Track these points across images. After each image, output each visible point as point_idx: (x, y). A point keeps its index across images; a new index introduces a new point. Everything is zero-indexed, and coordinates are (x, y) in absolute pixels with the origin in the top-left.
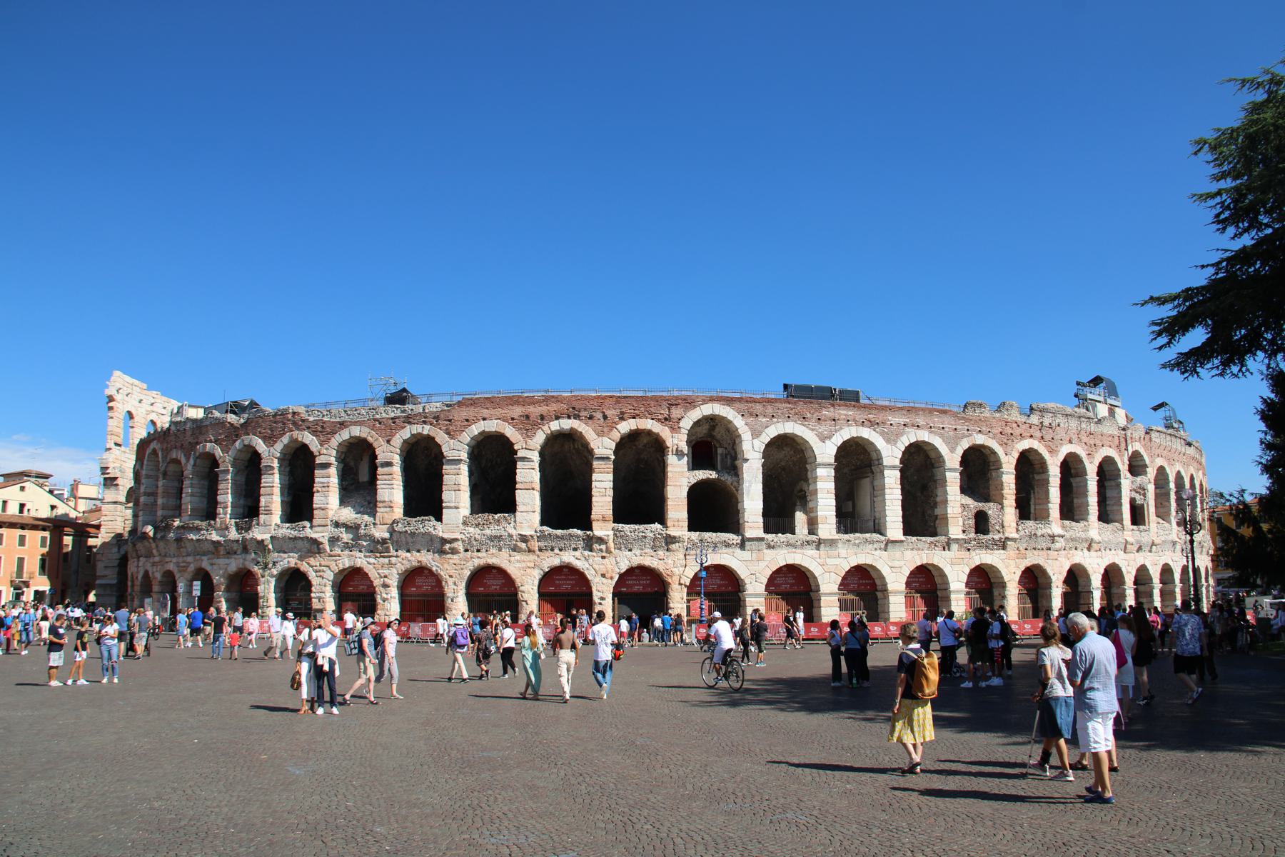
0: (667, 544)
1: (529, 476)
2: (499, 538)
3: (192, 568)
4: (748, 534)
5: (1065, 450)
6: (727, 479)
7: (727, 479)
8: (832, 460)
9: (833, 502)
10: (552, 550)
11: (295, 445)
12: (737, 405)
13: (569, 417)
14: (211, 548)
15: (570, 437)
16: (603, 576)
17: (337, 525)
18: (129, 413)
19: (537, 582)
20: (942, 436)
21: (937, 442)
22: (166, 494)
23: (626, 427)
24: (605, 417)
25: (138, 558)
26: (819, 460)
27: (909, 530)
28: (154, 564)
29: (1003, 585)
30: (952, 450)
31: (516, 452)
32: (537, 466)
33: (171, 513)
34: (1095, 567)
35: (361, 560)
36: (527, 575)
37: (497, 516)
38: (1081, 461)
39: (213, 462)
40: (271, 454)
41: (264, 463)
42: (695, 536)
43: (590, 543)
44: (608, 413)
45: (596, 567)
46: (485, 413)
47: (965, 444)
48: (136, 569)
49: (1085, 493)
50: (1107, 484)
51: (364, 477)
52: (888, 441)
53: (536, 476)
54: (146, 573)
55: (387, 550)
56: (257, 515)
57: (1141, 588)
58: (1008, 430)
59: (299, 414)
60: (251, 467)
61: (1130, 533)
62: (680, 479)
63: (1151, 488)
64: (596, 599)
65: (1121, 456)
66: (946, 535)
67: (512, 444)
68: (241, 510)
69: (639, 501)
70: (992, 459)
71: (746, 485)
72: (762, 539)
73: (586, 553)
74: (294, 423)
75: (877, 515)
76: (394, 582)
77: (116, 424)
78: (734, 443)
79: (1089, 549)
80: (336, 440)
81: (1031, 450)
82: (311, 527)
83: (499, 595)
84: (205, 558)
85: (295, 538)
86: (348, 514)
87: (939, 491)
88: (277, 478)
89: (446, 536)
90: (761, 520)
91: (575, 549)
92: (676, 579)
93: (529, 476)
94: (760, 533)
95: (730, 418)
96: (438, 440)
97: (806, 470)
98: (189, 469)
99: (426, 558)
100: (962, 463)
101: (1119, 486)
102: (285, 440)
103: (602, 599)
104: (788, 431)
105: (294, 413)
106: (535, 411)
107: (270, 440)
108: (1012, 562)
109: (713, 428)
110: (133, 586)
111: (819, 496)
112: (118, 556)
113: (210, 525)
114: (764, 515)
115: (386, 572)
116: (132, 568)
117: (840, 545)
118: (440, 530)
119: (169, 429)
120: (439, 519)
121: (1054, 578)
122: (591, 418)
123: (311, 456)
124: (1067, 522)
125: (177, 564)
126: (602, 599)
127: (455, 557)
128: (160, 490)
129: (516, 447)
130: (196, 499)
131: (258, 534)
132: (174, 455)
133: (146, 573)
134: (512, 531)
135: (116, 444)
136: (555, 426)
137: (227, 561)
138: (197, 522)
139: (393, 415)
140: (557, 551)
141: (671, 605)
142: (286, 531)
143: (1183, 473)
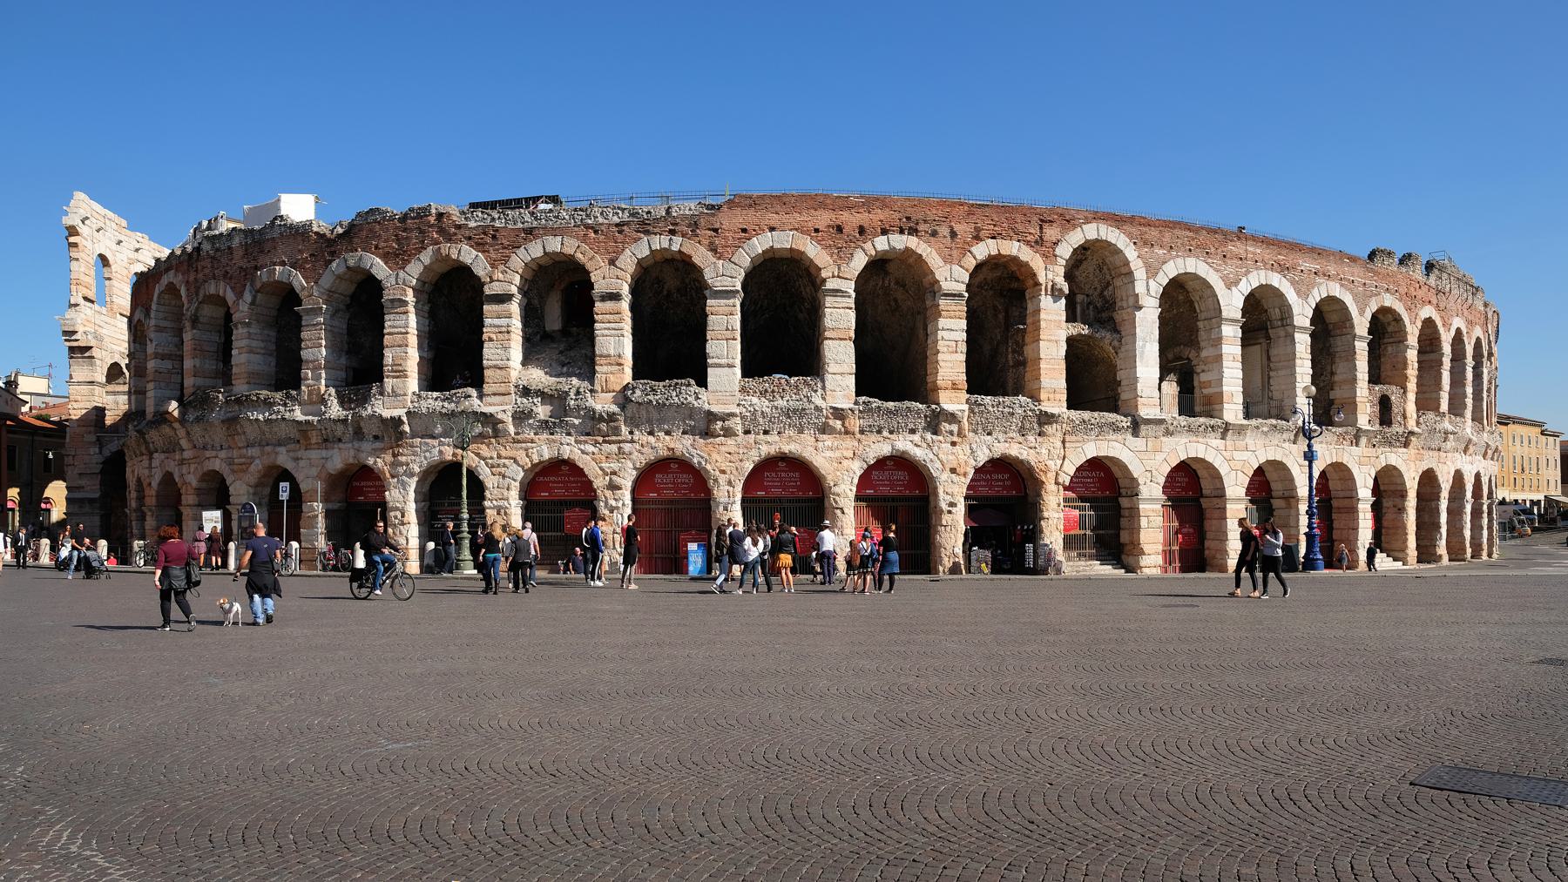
0: (1041, 424)
1: (840, 317)
2: (801, 412)
3: (257, 467)
6: (1105, 336)
10: (879, 432)
11: (444, 268)
12: (1127, 227)
13: (902, 232)
14: (294, 434)
16: (953, 471)
17: (526, 392)
18: (103, 258)
21: (1348, 300)
22: (198, 350)
23: (982, 251)
24: (953, 234)
26: (1224, 314)
28: (182, 462)
31: (824, 281)
32: (851, 302)
33: (208, 382)
36: (841, 466)
37: (793, 380)
39: (289, 297)
40: (402, 284)
41: (388, 295)
42: (1074, 414)
43: (935, 421)
44: (957, 228)
46: (773, 219)
47: (1373, 307)
48: (143, 471)
52: (1298, 293)
53: (851, 318)
55: (617, 431)
56: (380, 378)
59: (449, 215)
62: (1053, 331)
66: (1354, 423)
68: (343, 375)
71: (1139, 343)
73: (929, 436)
74: (442, 231)
76: (627, 482)
77: (83, 269)
80: (519, 260)
82: (481, 397)
83: (789, 501)
84: (282, 450)
85: (453, 414)
86: (538, 377)
88: (412, 319)
91: (913, 431)
92: (1051, 476)
93: (840, 317)
95: (1120, 245)
96: (697, 260)
98: (242, 310)
102: (426, 257)
103: (952, 504)
105: (440, 216)
106: (851, 219)
107: (397, 258)
113: (288, 396)
115: (615, 466)
116: (135, 469)
118: (708, 400)
120: (703, 383)
122: (934, 234)
125: (230, 462)
126: (952, 504)
127: (730, 441)
128: (188, 346)
129: (824, 274)
131: (382, 408)
132: (211, 289)
134: (818, 401)
135: (86, 299)
136: (882, 243)
137: (324, 453)
138: (264, 393)
139: (616, 220)
140: (885, 433)
141: (1046, 514)
142: (433, 402)
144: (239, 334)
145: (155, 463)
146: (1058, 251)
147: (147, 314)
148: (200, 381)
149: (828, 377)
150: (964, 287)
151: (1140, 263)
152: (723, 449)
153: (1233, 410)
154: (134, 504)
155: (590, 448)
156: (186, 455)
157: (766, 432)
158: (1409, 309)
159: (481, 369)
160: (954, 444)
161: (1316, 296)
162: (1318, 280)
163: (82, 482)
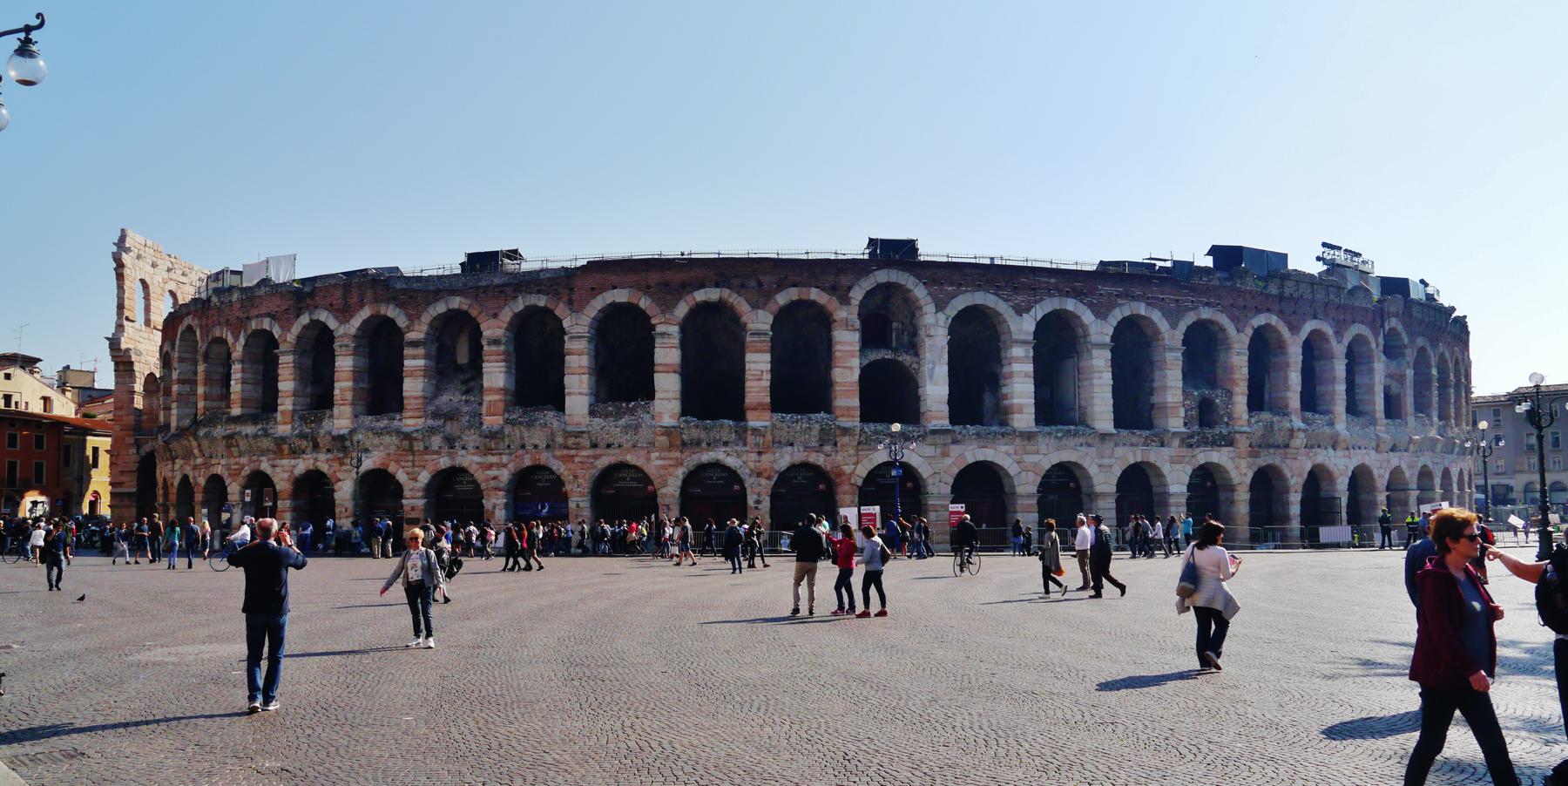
1: (667, 353)
3: (247, 471)
4: (934, 424)
5: (1309, 326)
7: (906, 359)
8: (1031, 337)
9: (1032, 388)
13: (717, 285)
15: (719, 307)
16: (759, 475)
19: (679, 483)
20: (1161, 309)
21: (1156, 316)
22: (208, 381)
23: (782, 299)
24: (760, 285)
25: (173, 460)
27: (1119, 422)
29: (1231, 488)
30: (1174, 326)
31: (653, 327)
32: (676, 341)
34: (1340, 465)
35: (468, 459)
38: (1327, 341)
40: (346, 330)
42: (870, 427)
44: (766, 279)
45: (752, 465)
46: (614, 278)
47: (1190, 319)
49: (1333, 380)
50: (1356, 368)
51: (463, 357)
54: (185, 478)
57: (1396, 495)
58: (1241, 302)
60: (319, 346)
61: (1383, 429)
63: (1410, 373)
64: (751, 502)
65: (1376, 335)
67: (649, 318)
69: (801, 388)
70: (1220, 336)
71: (926, 368)
72: (946, 432)
75: (1083, 403)
78: (913, 315)
79: (1334, 448)
81: (1267, 327)
87: (1157, 374)
89: (569, 429)
90: (946, 408)
91: (726, 444)
93: (667, 353)
94: (945, 423)
95: (910, 286)
96: (557, 312)
97: (999, 350)
98: (238, 351)
99: (545, 458)
100: (1185, 342)
101: (1371, 371)
102: (365, 313)
103: (758, 502)
104: (978, 302)
106: (677, 277)
108: (1243, 463)
109: (887, 298)
110: (166, 495)
111: (1015, 379)
112: (137, 458)
114: (949, 403)
116: (163, 471)
117: (1040, 439)
119: (209, 299)
120: (560, 406)
121: (1292, 482)
122: (742, 286)
123: (399, 333)
124: (1309, 415)
125: (228, 467)
128: (200, 377)
130: (249, 387)
133: (185, 478)
136: (701, 296)
142: (368, 420)
143: (1447, 354)
144: (236, 367)
145: (177, 467)
146: (851, 294)
147: (173, 348)
148: (209, 404)
149: (656, 402)
150: (768, 327)
151: (929, 299)
152: (577, 459)
153: (1024, 419)
154: (161, 500)
155: (477, 459)
156: (199, 461)
157: (609, 446)
158: (1232, 319)
159: (402, 398)
160: (760, 453)
161: (1117, 315)
162: (1120, 301)
163: (123, 479)
